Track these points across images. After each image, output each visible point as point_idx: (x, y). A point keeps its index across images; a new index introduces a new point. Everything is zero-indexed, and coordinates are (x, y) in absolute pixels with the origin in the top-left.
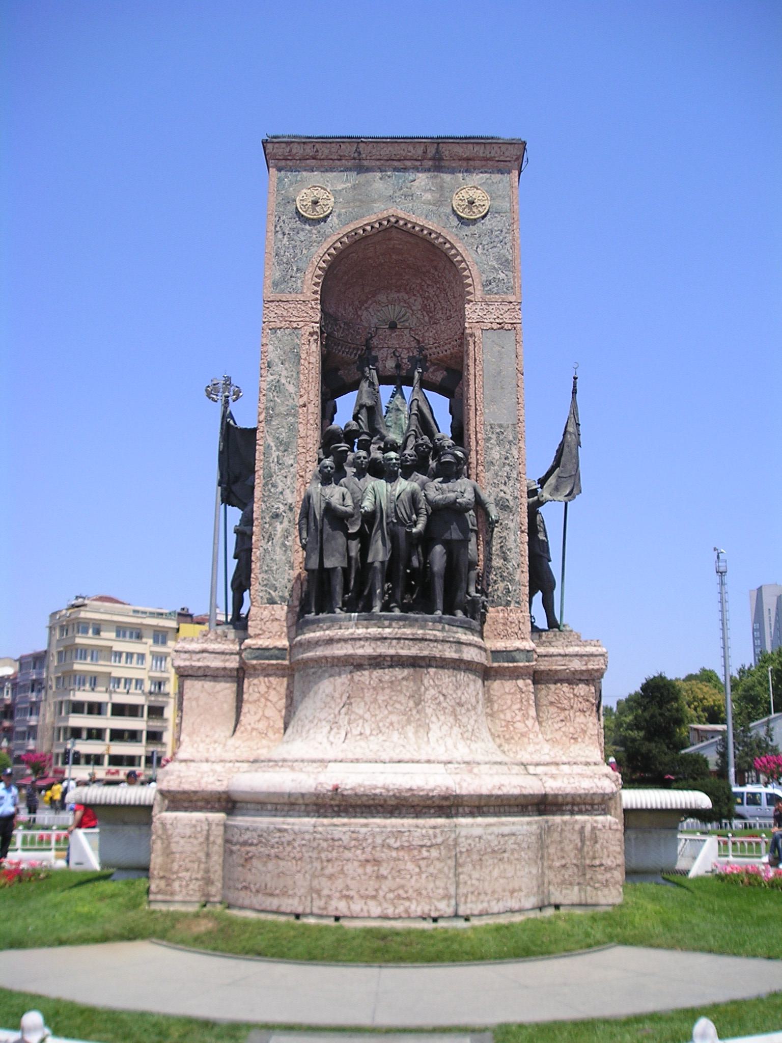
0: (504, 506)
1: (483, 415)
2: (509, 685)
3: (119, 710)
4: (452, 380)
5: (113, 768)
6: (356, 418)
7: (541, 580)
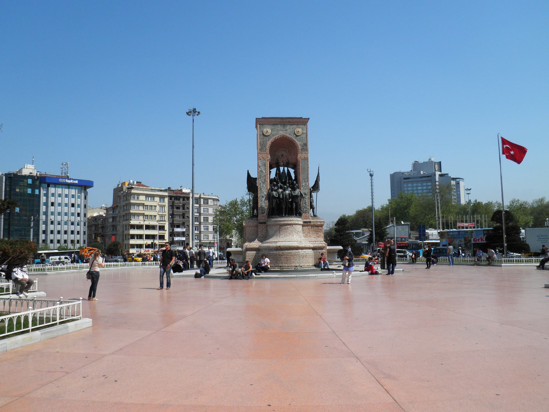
0: (305, 194)
1: (301, 178)
2: (307, 228)
3: (148, 227)
4: (295, 166)
5: (147, 249)
6: (276, 175)
7: (312, 207)
